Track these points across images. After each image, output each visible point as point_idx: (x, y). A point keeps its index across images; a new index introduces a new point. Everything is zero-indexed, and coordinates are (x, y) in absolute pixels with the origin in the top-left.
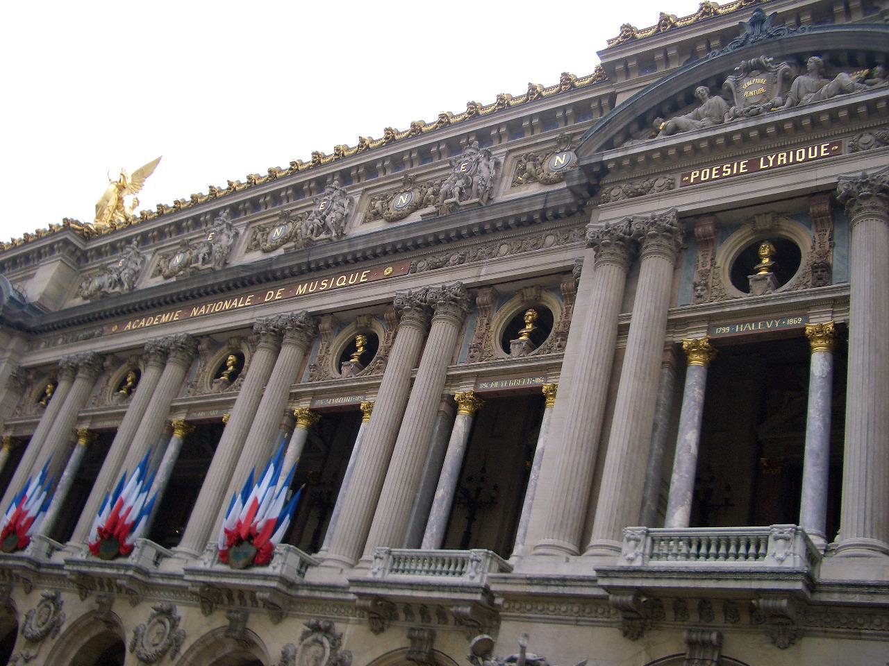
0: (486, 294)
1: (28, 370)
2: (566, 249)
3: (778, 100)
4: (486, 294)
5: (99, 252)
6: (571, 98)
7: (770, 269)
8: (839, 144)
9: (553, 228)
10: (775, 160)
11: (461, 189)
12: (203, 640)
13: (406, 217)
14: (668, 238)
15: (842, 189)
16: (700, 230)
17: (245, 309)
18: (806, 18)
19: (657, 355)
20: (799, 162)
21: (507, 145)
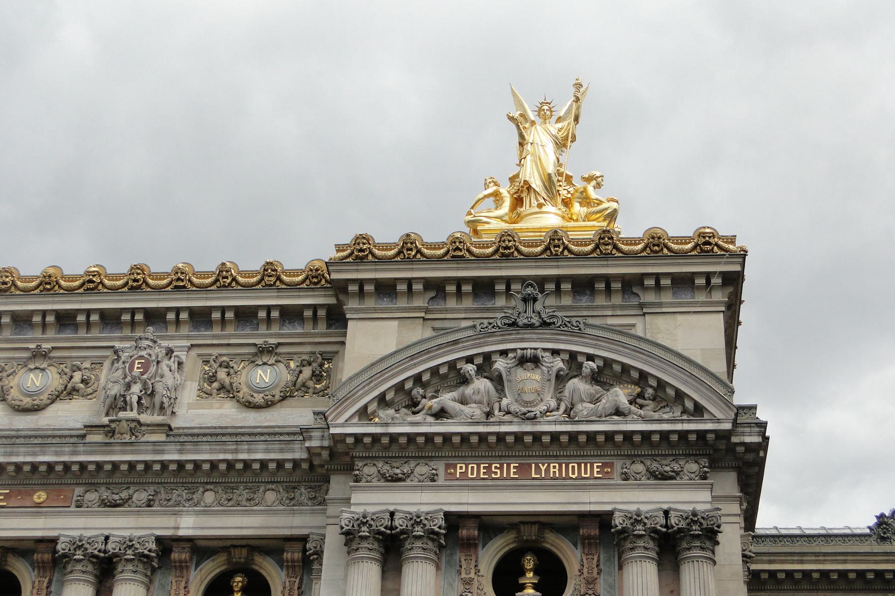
0: (184, 548)
2: (293, 512)
3: (553, 404)
4: (184, 548)
6: (278, 297)
7: (536, 587)
8: (611, 465)
9: (274, 482)
10: (547, 470)
11: (140, 398)
13: (43, 409)
14: (433, 540)
15: (618, 521)
16: (464, 532)
18: (566, 286)
20: (572, 478)
21: (188, 337)
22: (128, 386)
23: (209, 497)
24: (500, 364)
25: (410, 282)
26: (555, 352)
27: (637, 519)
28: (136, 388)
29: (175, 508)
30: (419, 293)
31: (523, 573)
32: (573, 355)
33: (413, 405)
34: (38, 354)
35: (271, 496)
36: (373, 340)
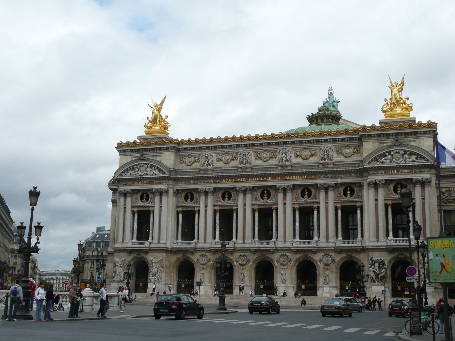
1: (178, 190)
5: (185, 149)
12: (297, 259)
15: (414, 180)
17: (269, 181)
18: (403, 134)
19: (384, 206)
22: (324, 156)
23: (342, 176)
24: (392, 153)
25: (374, 134)
26: (402, 150)
27: (417, 180)
28: (326, 156)
29: (336, 178)
30: (376, 137)
31: (398, 188)
32: (405, 150)
33: (377, 160)
34: (305, 148)
35: (353, 175)
36: (369, 146)
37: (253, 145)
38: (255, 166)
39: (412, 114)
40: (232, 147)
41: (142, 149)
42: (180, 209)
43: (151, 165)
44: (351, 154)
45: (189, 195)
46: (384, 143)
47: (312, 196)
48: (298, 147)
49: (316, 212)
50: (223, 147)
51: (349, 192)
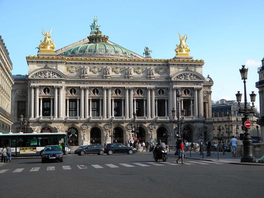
18: (189, 65)
35: (164, 84)
37: (111, 64)
38: (112, 76)
39: (190, 55)
40: (99, 64)
41: (44, 61)
42: (68, 98)
43: (52, 71)
44: (163, 72)
45: (73, 90)
46: (180, 68)
47: (143, 94)
48: (136, 67)
49: (145, 102)
50: (94, 64)
51: (161, 92)
